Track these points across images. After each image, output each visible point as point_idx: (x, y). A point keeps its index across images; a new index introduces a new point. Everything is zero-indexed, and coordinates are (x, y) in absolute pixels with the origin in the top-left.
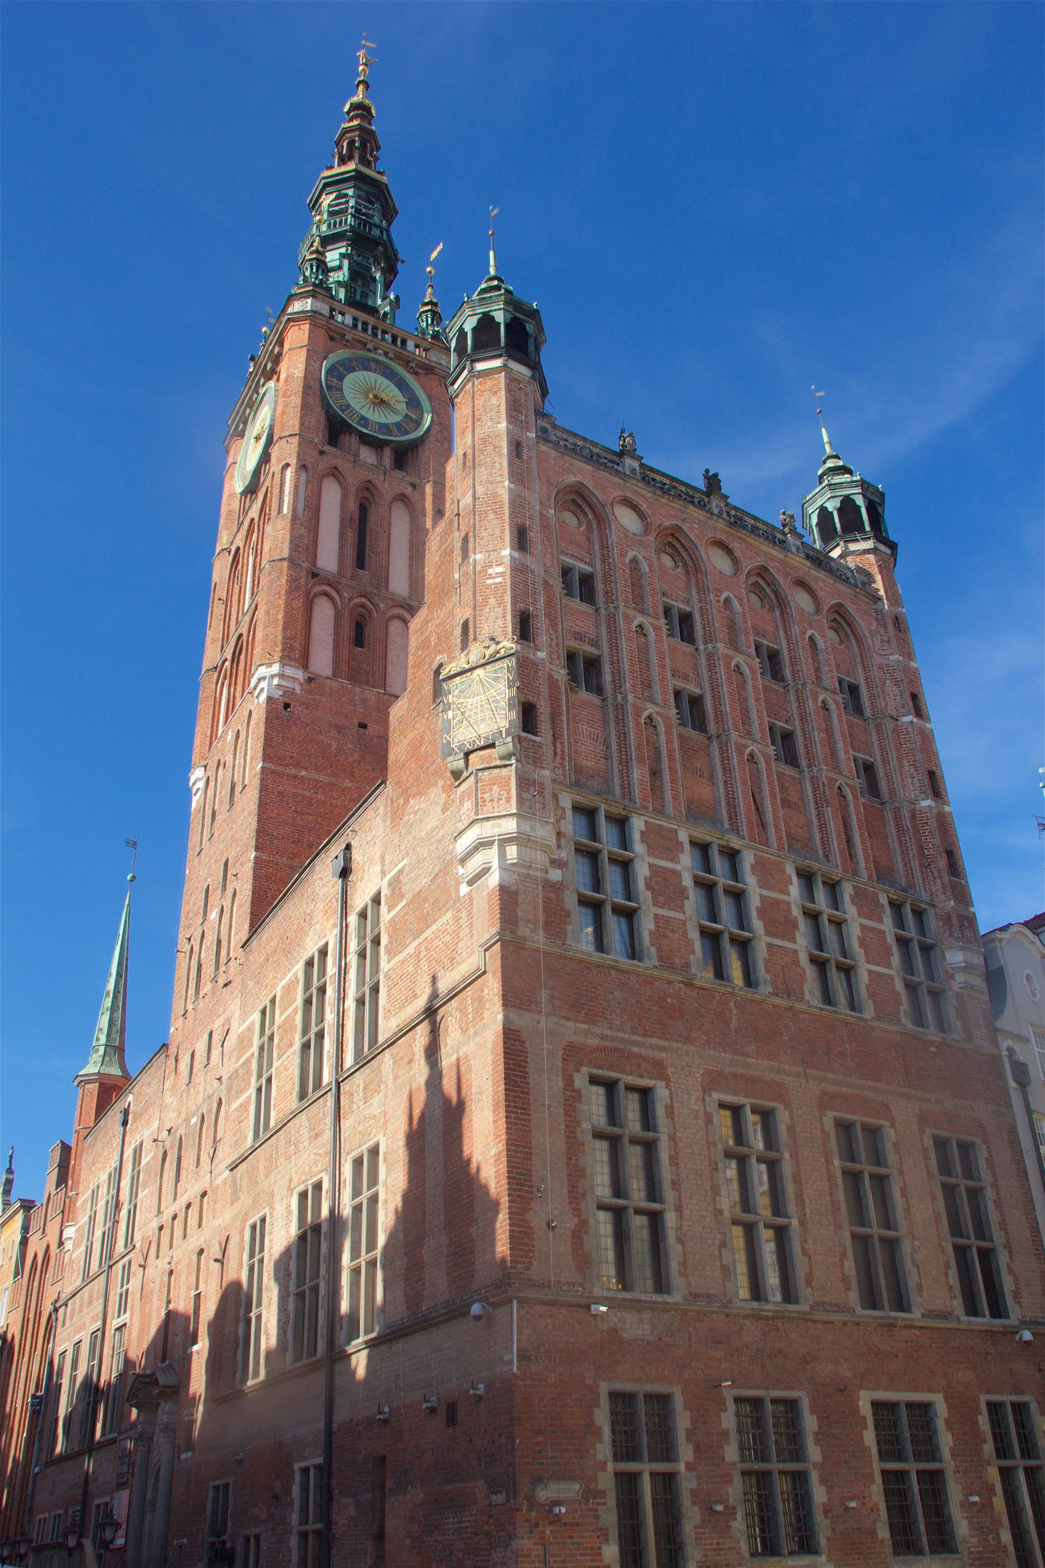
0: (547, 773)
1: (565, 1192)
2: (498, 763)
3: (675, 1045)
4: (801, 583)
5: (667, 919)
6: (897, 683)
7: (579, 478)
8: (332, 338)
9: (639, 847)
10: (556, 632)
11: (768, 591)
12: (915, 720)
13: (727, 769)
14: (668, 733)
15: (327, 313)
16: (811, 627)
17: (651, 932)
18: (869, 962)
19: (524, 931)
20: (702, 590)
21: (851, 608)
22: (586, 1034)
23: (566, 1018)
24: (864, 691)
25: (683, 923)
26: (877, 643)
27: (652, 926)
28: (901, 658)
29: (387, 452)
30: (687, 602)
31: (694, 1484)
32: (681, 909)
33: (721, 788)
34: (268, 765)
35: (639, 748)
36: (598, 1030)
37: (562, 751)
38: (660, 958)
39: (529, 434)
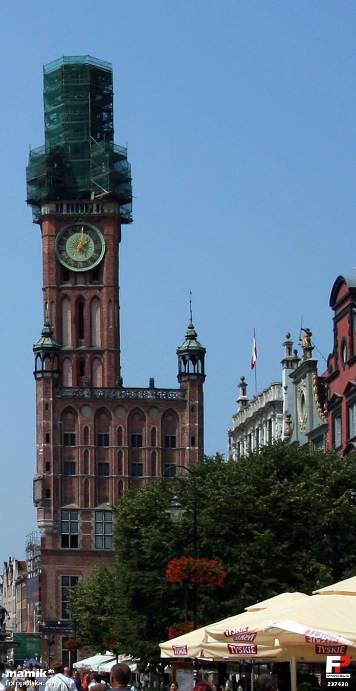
0: (52, 508)
1: (54, 600)
2: (41, 507)
3: (85, 566)
4: (153, 407)
5: (86, 536)
7: (69, 405)
8: (60, 221)
9: (79, 518)
11: (141, 414)
15: (54, 210)
16: (153, 424)
19: (47, 547)
21: (174, 408)
22: (62, 567)
23: (57, 564)
24: (177, 439)
25: (90, 536)
27: (81, 539)
29: (88, 276)
31: (80, 653)
32: (90, 533)
35: (81, 491)
36: (65, 566)
38: (83, 546)
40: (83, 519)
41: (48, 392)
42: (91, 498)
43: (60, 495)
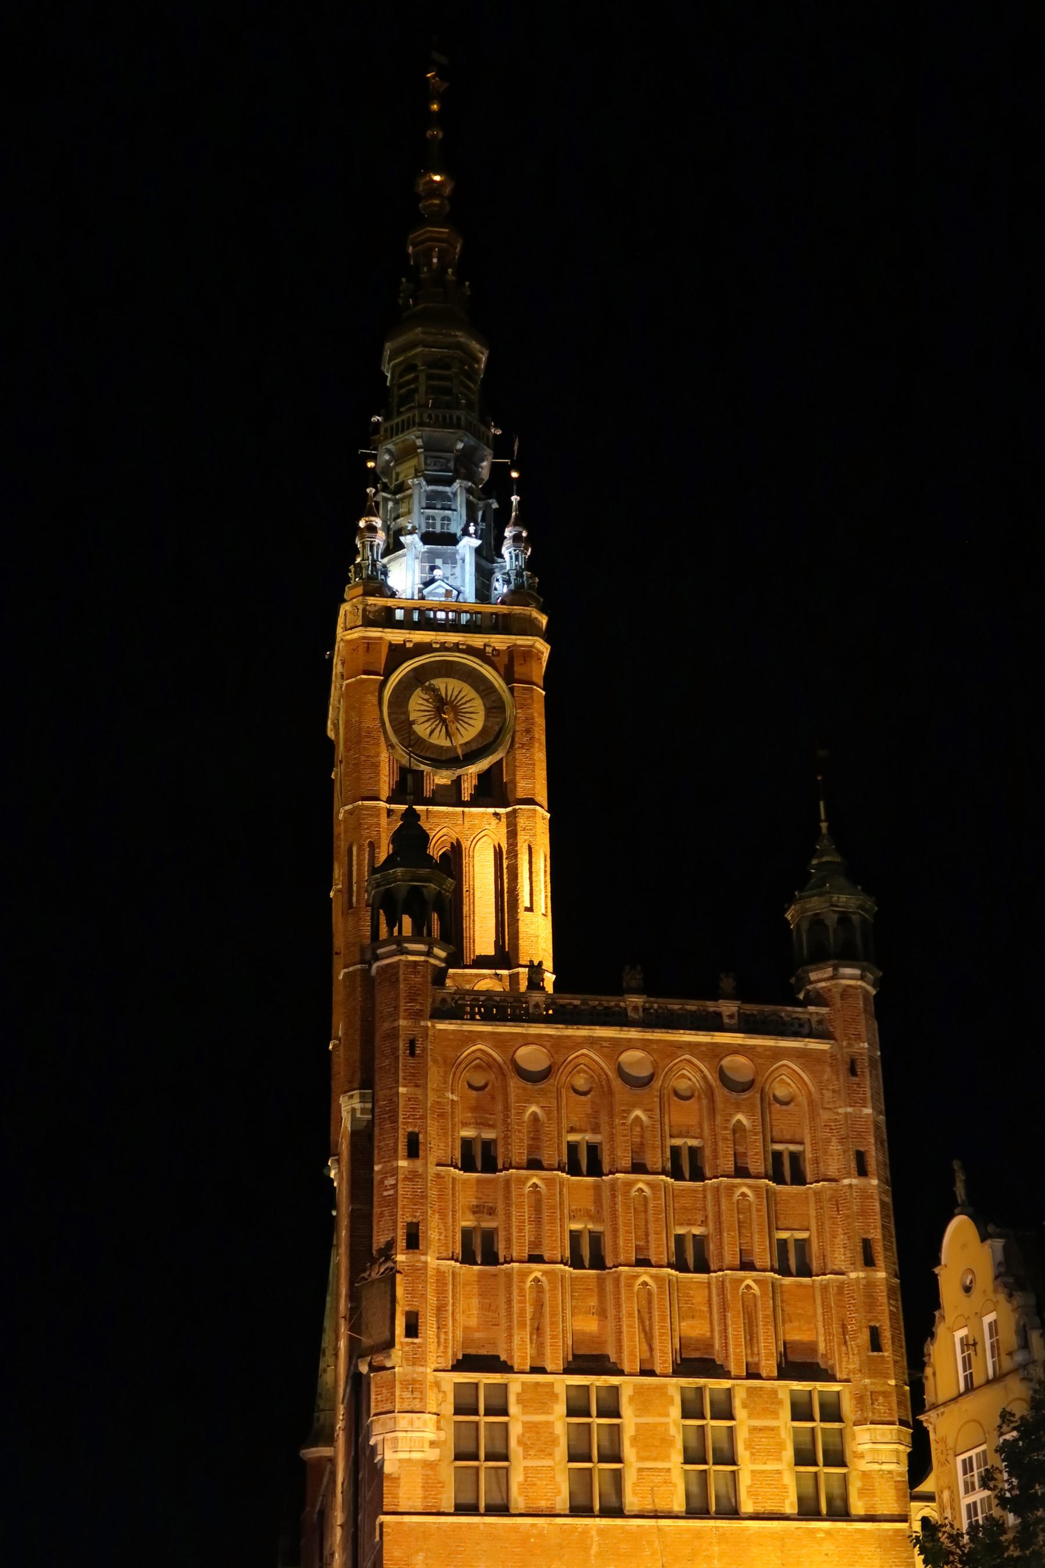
5: (537, 1470)
6: (842, 1140)
10: (445, 1224)
12: (855, 1181)
13: (618, 1305)
14: (553, 1289)
17: (520, 1484)
18: (753, 1463)
20: (611, 1115)
26: (827, 1094)
28: (849, 1110)
30: (596, 1130)
33: (611, 1324)
34: (358, 1206)
37: (446, 1339)
39: (422, 1023)
40: (524, 1414)
41: (412, 1000)
42: (553, 1337)
43: (451, 1329)
